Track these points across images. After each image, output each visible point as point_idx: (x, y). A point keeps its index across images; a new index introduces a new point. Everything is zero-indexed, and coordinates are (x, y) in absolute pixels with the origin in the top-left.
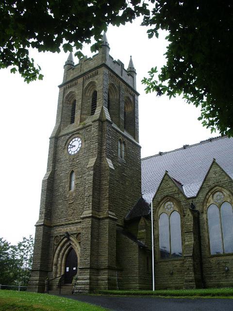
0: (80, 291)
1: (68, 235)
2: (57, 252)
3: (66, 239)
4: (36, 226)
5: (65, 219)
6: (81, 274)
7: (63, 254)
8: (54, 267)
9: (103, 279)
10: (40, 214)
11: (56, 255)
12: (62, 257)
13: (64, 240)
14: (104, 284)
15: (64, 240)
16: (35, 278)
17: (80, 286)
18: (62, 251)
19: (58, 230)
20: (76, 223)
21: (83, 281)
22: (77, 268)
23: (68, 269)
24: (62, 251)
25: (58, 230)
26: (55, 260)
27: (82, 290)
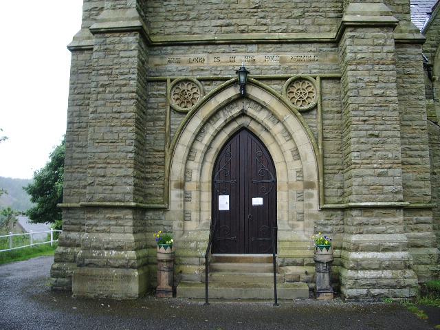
0: (376, 291)
1: (245, 81)
2: (187, 137)
3: (232, 92)
4: (75, 50)
5: (219, 22)
6: (364, 229)
7: (209, 147)
8: (174, 194)
9: (420, 242)
10: (73, 73)
11: (181, 151)
12: (204, 160)
13: (222, 98)
14: (426, 260)
15: (222, 98)
16: (105, 237)
17: (374, 274)
18: (206, 139)
19: (183, 58)
20: (281, 42)
21: (380, 255)
22: (215, 203)
23: (224, 202)
24: (206, 139)
25: (183, 58)
26: (177, 168)
27: (386, 286)
